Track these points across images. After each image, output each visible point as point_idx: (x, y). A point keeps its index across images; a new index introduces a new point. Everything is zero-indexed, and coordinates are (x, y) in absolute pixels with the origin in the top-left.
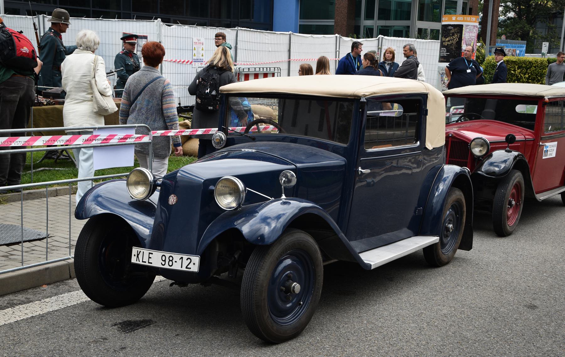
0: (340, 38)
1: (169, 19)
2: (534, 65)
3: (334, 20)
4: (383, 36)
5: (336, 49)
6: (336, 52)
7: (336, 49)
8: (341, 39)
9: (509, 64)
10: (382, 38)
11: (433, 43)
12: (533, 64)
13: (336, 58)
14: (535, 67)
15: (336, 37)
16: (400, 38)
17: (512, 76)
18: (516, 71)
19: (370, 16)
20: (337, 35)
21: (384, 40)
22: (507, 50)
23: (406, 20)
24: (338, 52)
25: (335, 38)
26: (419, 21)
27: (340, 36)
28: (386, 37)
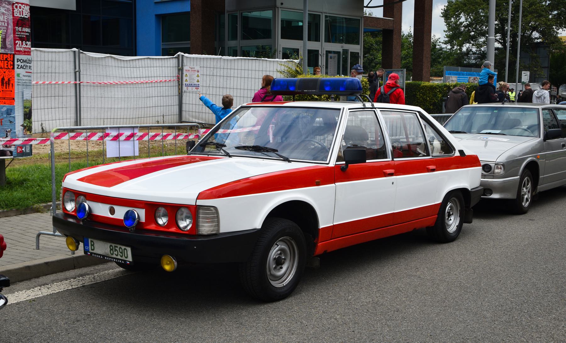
0: (79, 53)
3: (189, 42)
4: (183, 54)
5: (75, 68)
6: (75, 73)
7: (75, 68)
8: (81, 55)
10: (183, 56)
11: (243, 61)
13: (76, 80)
15: (75, 52)
19: (234, 37)
20: (75, 49)
21: (185, 60)
22: (472, 78)
24: (78, 73)
25: (72, 54)
26: (308, 41)
28: (186, 55)
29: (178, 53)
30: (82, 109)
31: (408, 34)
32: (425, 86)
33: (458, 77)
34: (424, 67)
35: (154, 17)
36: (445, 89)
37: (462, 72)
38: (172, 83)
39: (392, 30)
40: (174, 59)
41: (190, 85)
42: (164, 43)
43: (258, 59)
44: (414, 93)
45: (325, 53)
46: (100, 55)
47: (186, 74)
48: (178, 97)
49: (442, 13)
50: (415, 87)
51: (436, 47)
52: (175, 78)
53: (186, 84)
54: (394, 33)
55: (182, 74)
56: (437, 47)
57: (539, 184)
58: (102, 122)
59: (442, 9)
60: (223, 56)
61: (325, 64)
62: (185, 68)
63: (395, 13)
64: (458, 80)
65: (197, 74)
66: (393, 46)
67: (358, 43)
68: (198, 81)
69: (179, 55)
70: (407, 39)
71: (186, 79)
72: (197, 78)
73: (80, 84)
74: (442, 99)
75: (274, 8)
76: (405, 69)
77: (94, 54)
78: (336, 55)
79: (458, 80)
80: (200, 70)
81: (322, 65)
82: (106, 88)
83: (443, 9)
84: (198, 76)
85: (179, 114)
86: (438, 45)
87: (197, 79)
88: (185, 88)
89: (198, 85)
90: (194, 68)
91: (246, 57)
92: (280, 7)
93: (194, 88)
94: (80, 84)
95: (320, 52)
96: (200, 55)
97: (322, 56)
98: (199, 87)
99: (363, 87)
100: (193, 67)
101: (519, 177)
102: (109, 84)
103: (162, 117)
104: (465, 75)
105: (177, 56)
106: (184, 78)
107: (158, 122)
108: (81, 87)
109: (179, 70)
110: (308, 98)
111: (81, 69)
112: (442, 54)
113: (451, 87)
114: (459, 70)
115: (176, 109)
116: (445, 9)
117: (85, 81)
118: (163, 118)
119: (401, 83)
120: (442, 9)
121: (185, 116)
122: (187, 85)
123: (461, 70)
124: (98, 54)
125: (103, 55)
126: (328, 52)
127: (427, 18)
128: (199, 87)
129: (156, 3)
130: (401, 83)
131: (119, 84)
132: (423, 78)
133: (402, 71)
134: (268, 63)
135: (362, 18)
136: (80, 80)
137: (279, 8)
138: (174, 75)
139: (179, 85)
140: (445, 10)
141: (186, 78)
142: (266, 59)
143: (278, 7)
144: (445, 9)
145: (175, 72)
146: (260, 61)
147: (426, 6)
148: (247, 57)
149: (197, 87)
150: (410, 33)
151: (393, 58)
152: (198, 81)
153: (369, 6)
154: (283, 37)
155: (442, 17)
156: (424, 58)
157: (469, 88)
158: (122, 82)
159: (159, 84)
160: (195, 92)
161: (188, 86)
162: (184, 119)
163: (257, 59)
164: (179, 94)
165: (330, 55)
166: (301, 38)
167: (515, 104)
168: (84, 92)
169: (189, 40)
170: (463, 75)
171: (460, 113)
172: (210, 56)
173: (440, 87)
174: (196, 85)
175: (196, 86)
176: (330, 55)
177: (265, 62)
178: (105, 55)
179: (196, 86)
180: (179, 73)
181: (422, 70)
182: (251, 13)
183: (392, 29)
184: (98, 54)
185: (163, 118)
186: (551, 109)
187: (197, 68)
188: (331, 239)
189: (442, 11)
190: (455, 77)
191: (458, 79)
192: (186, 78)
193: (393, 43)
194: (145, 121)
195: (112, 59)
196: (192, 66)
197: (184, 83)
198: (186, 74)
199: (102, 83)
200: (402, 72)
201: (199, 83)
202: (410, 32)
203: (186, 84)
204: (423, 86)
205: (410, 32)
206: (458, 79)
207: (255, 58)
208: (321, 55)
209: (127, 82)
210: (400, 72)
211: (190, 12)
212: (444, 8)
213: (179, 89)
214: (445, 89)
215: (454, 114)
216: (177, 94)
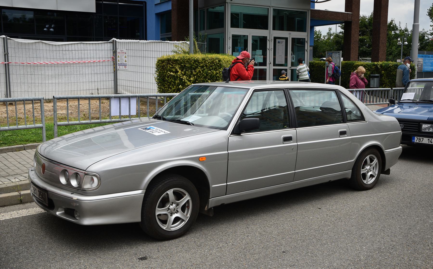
1: (18, 37)
2: (201, 65)
3: (171, 33)
5: (5, 52)
6: (5, 55)
8: (9, 41)
9: (170, 64)
12: (199, 62)
13: (5, 61)
14: (202, 67)
15: (4, 38)
16: (141, 41)
17: (175, 80)
18: (178, 72)
20: (4, 36)
21: (117, 44)
23: (219, 27)
27: (6, 37)
29: (113, 39)
30: (11, 84)
31: (404, 29)
32: (358, 65)
33: (424, 59)
34: (381, 50)
35: (155, 14)
36: (373, 67)
37: (428, 55)
38: (107, 63)
39: (350, 21)
40: (109, 44)
41: (121, 64)
42: (162, 34)
43: (163, 41)
44: (349, 71)
45: (273, 39)
46: (29, 41)
47: (118, 56)
48: (113, 74)
49: (428, 12)
50: (350, 66)
51: (425, 38)
52: (110, 60)
53: (118, 64)
54: (353, 24)
55: (116, 55)
56: (426, 38)
57: (210, 197)
58: (149, 91)
59: (428, 10)
60: (140, 40)
61: (273, 47)
62: (118, 51)
63: (353, 9)
64: (424, 61)
65: (125, 55)
66: (352, 34)
67: (305, 31)
68: (126, 61)
69: (113, 40)
70: (404, 32)
71: (120, 60)
72: (125, 59)
73: (8, 64)
74: (370, 75)
75: (224, 3)
76: (341, 51)
77: (23, 40)
78: (284, 40)
79: (424, 61)
80: (126, 53)
81: (271, 48)
82: (46, 68)
83: (429, 9)
84: (125, 57)
85: (115, 88)
86: (426, 36)
87: (125, 59)
88: (118, 67)
89: (126, 65)
90: (123, 51)
91: (151, 40)
92: (230, 3)
93: (124, 66)
94: (8, 64)
95: (268, 38)
96: (126, 40)
97: (270, 41)
98: (126, 65)
99: (217, 64)
100: (122, 49)
101: (140, 192)
102: (56, 64)
103: (97, 90)
104: (431, 57)
105: (112, 41)
106: (118, 59)
107: (92, 94)
108: (10, 67)
109: (114, 52)
110: (167, 75)
111: (9, 52)
112: (429, 42)
113: (378, 66)
114: (425, 53)
115: (112, 84)
116: (430, 9)
117: (14, 61)
118: (98, 91)
119: (338, 63)
120: (428, 10)
121: (120, 89)
122: (119, 64)
123: (427, 54)
124: (27, 40)
125: (33, 41)
126: (275, 38)
127: (383, 12)
128: (126, 65)
129: (156, 5)
130: (338, 63)
131: (50, 64)
132: (379, 59)
133: (339, 52)
134: (170, 45)
135: (309, 10)
136: (8, 61)
137: (229, 3)
138: (109, 56)
139: (114, 64)
140: (430, 10)
141: (119, 59)
142: (168, 41)
143: (228, 3)
144: (430, 9)
145: (111, 54)
146: (165, 43)
147: (382, 3)
148: (154, 40)
149: (125, 65)
150: (406, 28)
151: (352, 44)
152: (126, 61)
153: (318, 1)
154: (232, 26)
155: (428, 15)
156: (380, 43)
157: (392, 67)
158: (53, 62)
159: (92, 64)
160: (121, 70)
161: (120, 65)
162: (119, 92)
163: (162, 42)
164: (114, 71)
165: (277, 40)
166: (266, 27)
167: (266, 84)
168: (12, 69)
169: (171, 32)
170: (429, 57)
171: (216, 93)
172: (132, 40)
173: (368, 66)
174: (124, 65)
175: (125, 65)
176: (277, 40)
177: (167, 44)
178: (35, 41)
179: (125, 65)
180: (114, 55)
181: (379, 53)
182: (214, 9)
183: (351, 21)
184: (26, 40)
185: (98, 91)
186: (284, 90)
187: (125, 51)
188: (293, 182)
189: (428, 11)
190: (421, 59)
191: (424, 60)
192: (119, 59)
193: (352, 32)
194: (143, 92)
195: (43, 44)
196: (122, 49)
197: (118, 62)
198: (118, 56)
199: (32, 63)
200: (339, 53)
201: (126, 63)
202: (406, 27)
203: (118, 64)
204: (356, 65)
205: (406, 27)
206: (424, 60)
207: (161, 41)
208: (269, 40)
209: (41, 62)
210: (338, 54)
211: (171, 10)
212: (430, 9)
213: (114, 68)
214: (373, 67)
215: (179, 93)
216: (112, 71)
